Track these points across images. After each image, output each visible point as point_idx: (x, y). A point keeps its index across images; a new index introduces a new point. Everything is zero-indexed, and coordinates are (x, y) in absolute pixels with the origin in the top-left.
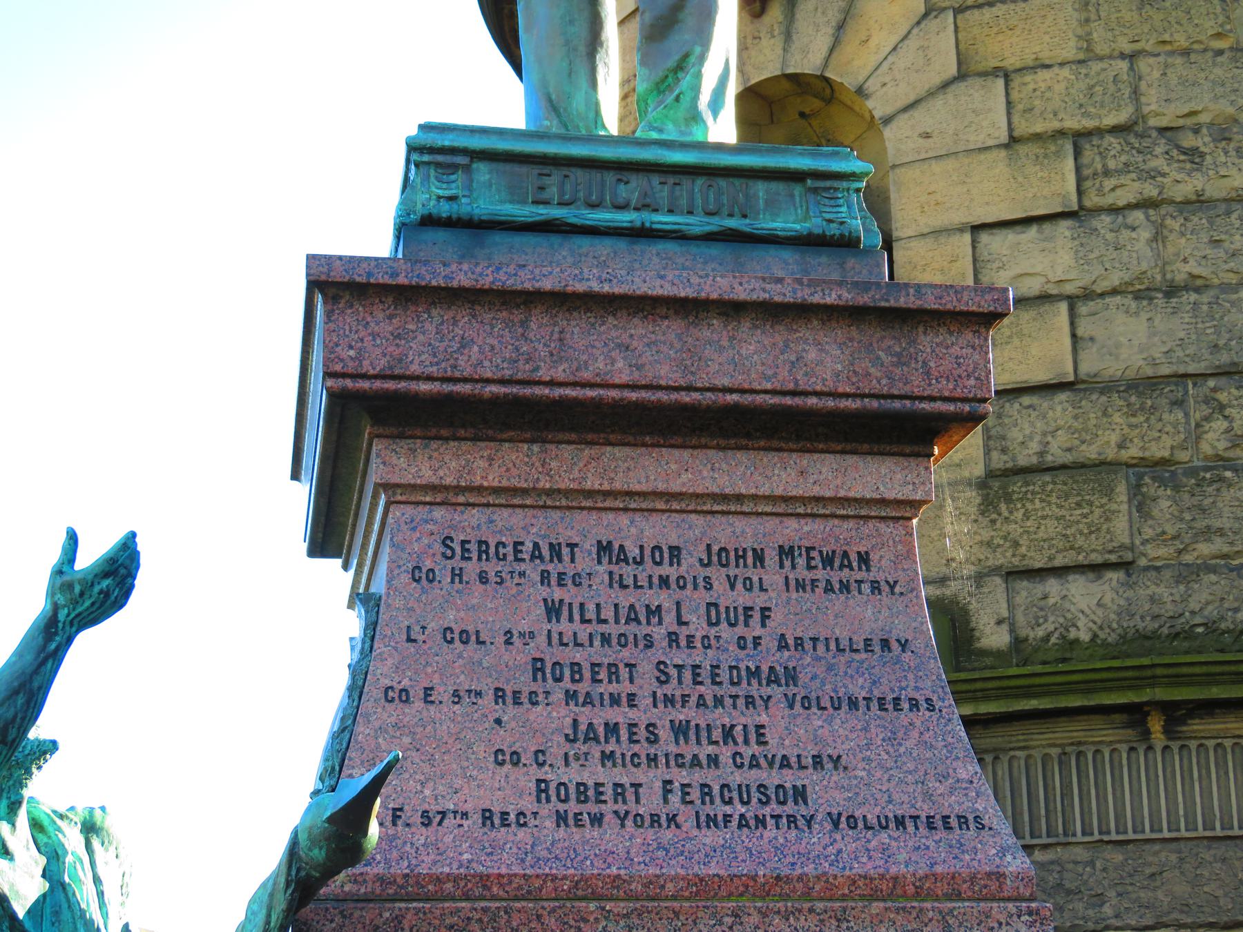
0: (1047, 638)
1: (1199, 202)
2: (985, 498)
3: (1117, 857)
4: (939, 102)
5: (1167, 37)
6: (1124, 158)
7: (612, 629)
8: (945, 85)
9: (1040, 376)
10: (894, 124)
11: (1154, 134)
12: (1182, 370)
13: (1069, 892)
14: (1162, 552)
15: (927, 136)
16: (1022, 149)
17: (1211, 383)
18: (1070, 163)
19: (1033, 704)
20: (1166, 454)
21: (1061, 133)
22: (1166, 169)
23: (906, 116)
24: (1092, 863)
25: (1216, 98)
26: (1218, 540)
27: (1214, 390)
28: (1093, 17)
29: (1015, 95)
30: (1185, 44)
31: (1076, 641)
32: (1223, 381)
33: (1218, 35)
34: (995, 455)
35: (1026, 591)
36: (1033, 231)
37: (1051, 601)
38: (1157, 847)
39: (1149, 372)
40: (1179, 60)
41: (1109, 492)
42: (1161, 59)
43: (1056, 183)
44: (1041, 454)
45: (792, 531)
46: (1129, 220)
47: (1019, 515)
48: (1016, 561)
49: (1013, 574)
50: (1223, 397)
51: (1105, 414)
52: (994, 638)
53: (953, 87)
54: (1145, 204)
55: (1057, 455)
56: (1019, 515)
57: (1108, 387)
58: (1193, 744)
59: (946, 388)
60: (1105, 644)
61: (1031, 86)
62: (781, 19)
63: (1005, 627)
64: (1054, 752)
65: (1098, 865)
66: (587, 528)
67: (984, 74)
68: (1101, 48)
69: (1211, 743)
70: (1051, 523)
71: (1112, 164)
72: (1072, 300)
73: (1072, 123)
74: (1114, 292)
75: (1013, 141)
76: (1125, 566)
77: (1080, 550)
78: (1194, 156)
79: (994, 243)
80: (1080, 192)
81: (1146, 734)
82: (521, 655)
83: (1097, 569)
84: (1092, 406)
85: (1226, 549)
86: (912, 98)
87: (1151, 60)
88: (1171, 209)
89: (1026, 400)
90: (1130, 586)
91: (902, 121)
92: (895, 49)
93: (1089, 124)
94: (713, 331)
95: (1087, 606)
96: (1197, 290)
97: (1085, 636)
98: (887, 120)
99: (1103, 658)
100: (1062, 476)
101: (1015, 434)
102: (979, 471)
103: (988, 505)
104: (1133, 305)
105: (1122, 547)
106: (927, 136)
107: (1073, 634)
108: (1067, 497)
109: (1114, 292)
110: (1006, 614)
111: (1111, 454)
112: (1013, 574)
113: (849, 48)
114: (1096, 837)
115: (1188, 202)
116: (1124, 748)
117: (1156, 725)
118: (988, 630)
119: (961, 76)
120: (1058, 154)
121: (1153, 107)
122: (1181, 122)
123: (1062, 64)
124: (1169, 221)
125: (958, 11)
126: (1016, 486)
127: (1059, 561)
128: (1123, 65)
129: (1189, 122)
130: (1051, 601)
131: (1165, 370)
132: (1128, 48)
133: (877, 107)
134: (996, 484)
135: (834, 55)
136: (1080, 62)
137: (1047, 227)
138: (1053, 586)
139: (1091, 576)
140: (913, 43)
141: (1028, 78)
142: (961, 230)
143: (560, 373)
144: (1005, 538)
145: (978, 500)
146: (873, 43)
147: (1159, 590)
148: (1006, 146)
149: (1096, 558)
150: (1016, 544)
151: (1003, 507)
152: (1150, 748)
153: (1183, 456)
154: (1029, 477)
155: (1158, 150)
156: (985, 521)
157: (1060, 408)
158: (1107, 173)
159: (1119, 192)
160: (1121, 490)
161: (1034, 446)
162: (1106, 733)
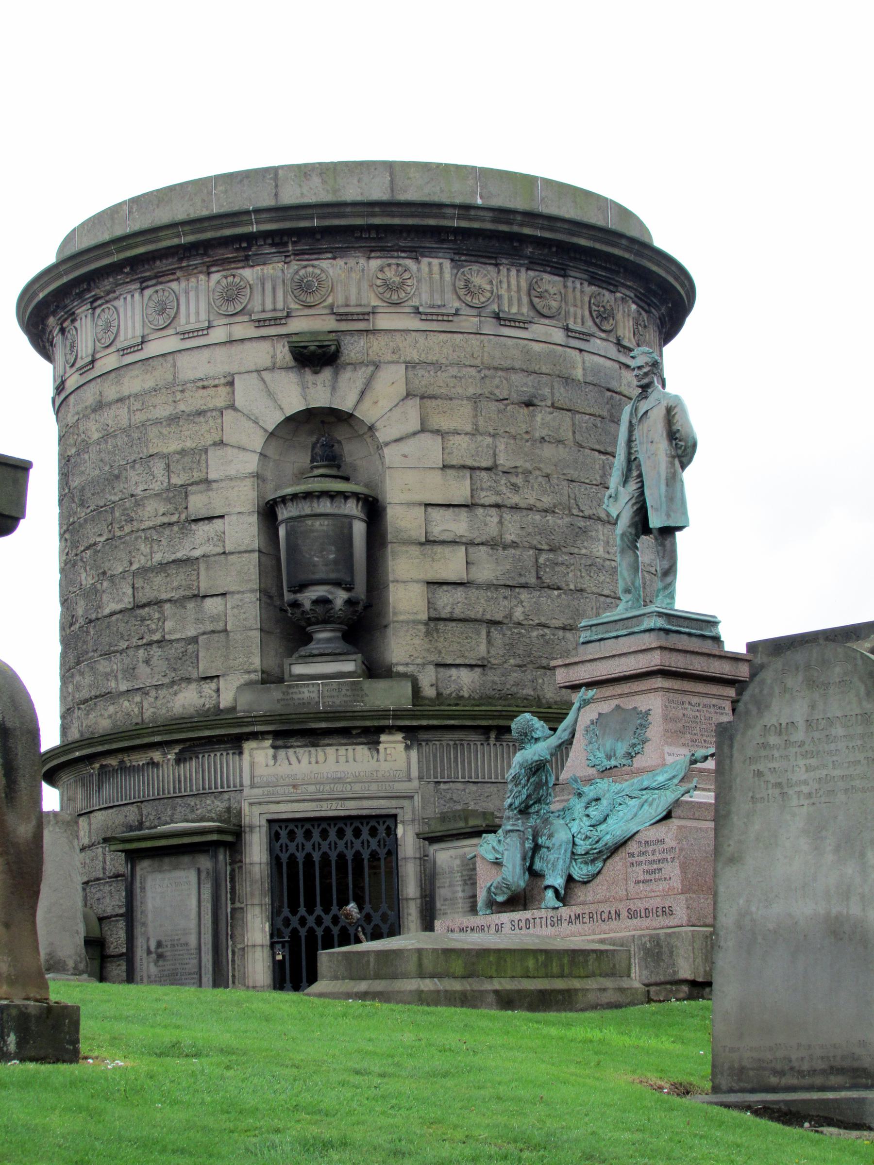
0: (450, 694)
1: (516, 508)
2: (427, 630)
3: (473, 788)
4: (412, 442)
5: (507, 430)
6: (489, 484)
7: (693, 720)
8: (415, 434)
9: (453, 578)
10: (389, 447)
11: (501, 473)
12: (508, 583)
13: (455, 802)
14: (496, 662)
15: (405, 456)
16: (450, 472)
17: (517, 590)
18: (468, 482)
19: (452, 722)
20: (500, 619)
21: (464, 467)
22: (505, 491)
23: (394, 444)
24: (464, 790)
25: (526, 461)
26: (518, 659)
27: (518, 593)
28: (479, 414)
29: (445, 445)
30: (514, 434)
31: (462, 696)
32: (522, 590)
33: (527, 432)
34: (431, 610)
35: (444, 673)
36: (451, 509)
37: (453, 678)
38: (489, 785)
39: (495, 582)
40: (512, 442)
41: (478, 633)
42: (505, 440)
43: (459, 489)
44: (451, 613)
45: (714, 701)
46: (490, 512)
47: (442, 639)
48: (440, 659)
49: (438, 665)
50: (523, 597)
51: (478, 598)
52: (429, 692)
53: (418, 436)
54: (497, 506)
55: (458, 613)
56: (442, 639)
57: (479, 586)
58: (505, 744)
59: (742, 675)
60: (474, 699)
61: (452, 442)
62: (330, 378)
63: (434, 688)
64: (452, 743)
65: (467, 791)
66: (686, 698)
67: (432, 432)
68: (481, 429)
69: (511, 744)
70: (455, 644)
71: (484, 486)
72: (466, 544)
73: (470, 462)
74: (482, 544)
75: (445, 467)
76: (483, 666)
77: (466, 658)
78: (515, 488)
79: (435, 513)
80: (472, 496)
81: (488, 738)
82: (680, 725)
83: (471, 666)
84: (473, 593)
85: (521, 663)
86: (398, 436)
87: (502, 440)
88: (505, 509)
89: (445, 588)
90: (484, 675)
91: (394, 446)
92: (391, 410)
93: (476, 464)
94: (711, 660)
95: (466, 681)
96: (514, 548)
97: (466, 695)
98: (387, 444)
99: (473, 705)
100: (461, 625)
101: (440, 603)
102: (424, 617)
103: (428, 633)
104: (491, 552)
105: (483, 658)
106: (405, 456)
107: (461, 693)
108: (462, 633)
109: (482, 544)
110: (434, 682)
111: (479, 616)
112: (438, 665)
113: (367, 403)
114: (467, 780)
115: (512, 508)
116: (479, 743)
117: (493, 736)
118: (427, 689)
119: (423, 430)
120: (463, 477)
121: (501, 462)
122: (511, 470)
123: (466, 434)
124: (505, 515)
125: (422, 397)
126: (441, 626)
127: (458, 662)
128: (489, 440)
129: (513, 470)
130: (453, 678)
131: (502, 583)
132: (492, 431)
133: (383, 435)
134: (432, 624)
135: (359, 405)
136: (473, 435)
137: (456, 510)
138: (454, 671)
139: (469, 669)
140: (399, 410)
141: (451, 438)
142: (420, 504)
143: (691, 667)
144: (435, 649)
145: (424, 630)
146: (380, 404)
147: (496, 678)
148: (442, 469)
149: (474, 663)
150: (440, 652)
151: (435, 635)
152: (488, 744)
153: (506, 621)
154: (448, 623)
155: (503, 482)
156: (427, 640)
157: (459, 594)
158: (482, 489)
159: (486, 499)
160: (484, 633)
161: (448, 609)
162: (474, 737)
